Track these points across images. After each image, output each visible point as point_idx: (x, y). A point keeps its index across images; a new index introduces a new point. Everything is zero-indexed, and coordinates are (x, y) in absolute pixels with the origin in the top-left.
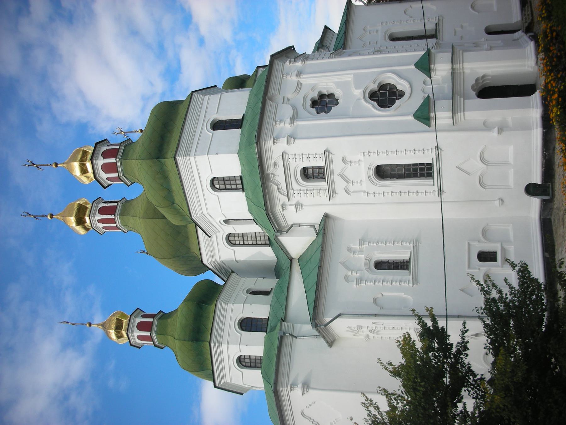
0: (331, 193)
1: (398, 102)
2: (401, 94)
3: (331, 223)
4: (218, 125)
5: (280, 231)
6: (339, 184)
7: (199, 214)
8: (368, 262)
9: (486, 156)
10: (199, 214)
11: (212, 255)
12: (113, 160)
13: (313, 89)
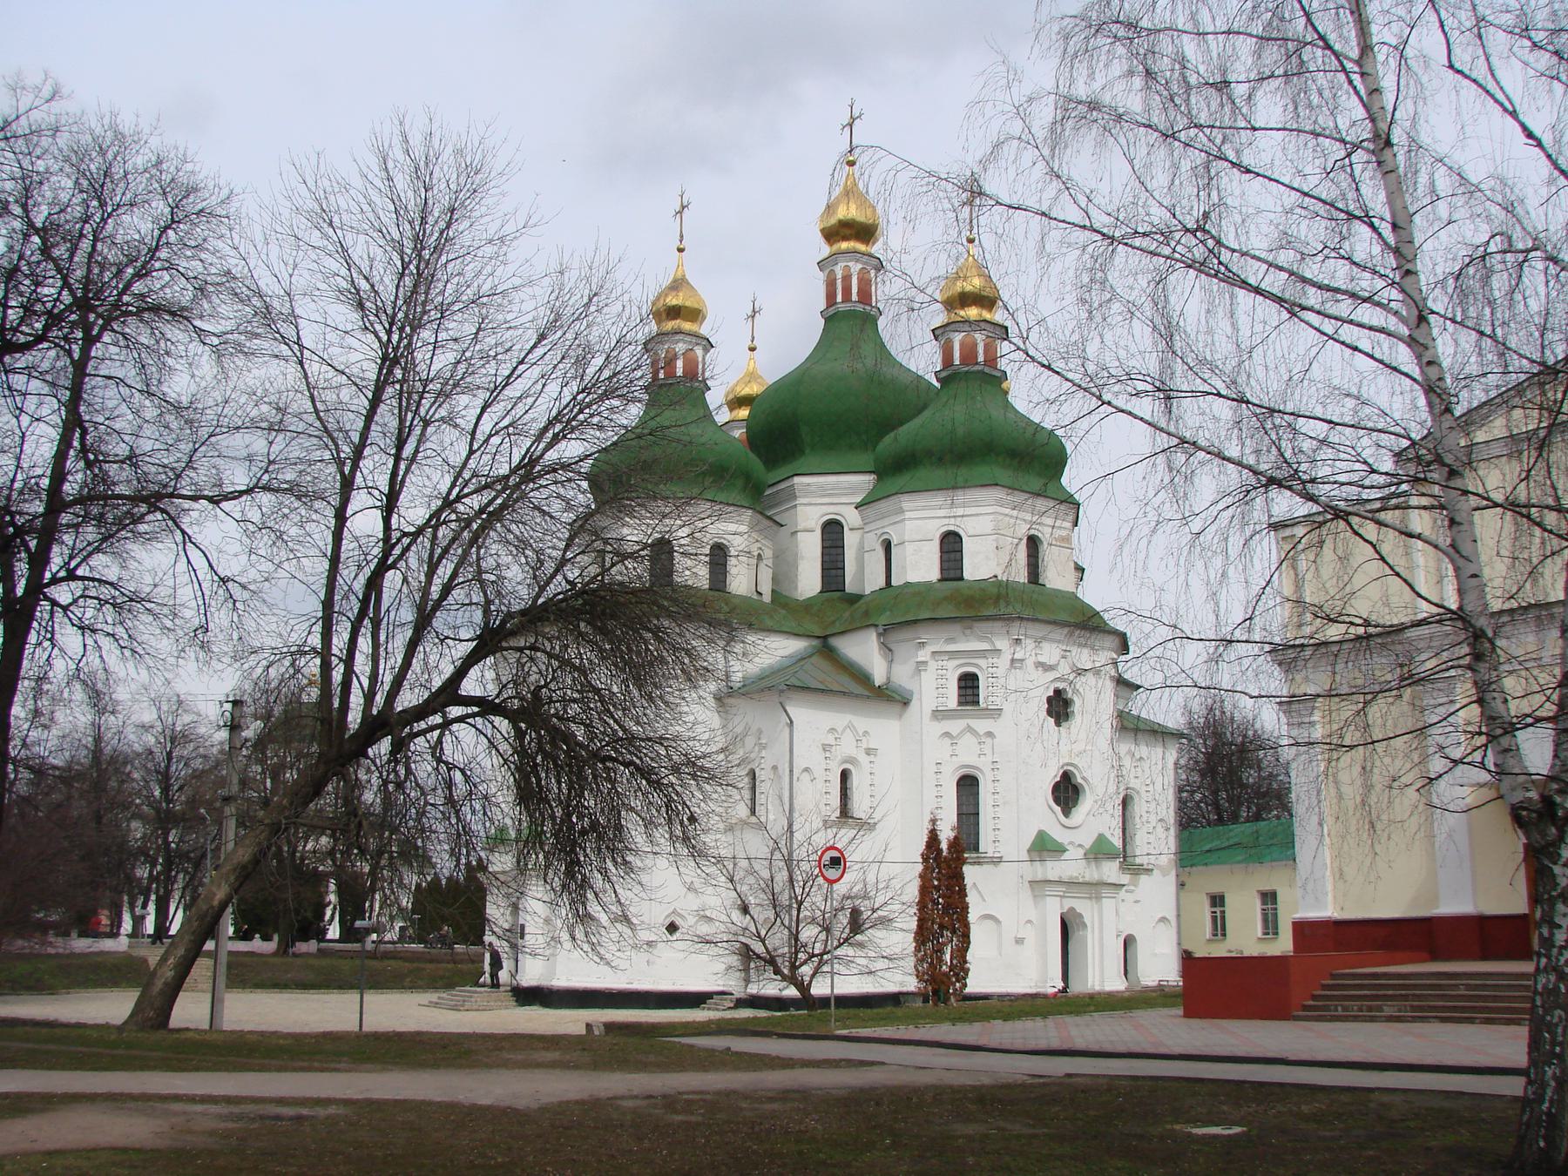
0: (939, 714)
1: (1058, 809)
2: (1067, 812)
3: (897, 708)
4: (1033, 543)
5: (886, 631)
6: (955, 726)
7: (905, 505)
8: (852, 760)
9: (989, 922)
10: (905, 505)
11: (808, 494)
12: (981, 358)
13: (1076, 691)
